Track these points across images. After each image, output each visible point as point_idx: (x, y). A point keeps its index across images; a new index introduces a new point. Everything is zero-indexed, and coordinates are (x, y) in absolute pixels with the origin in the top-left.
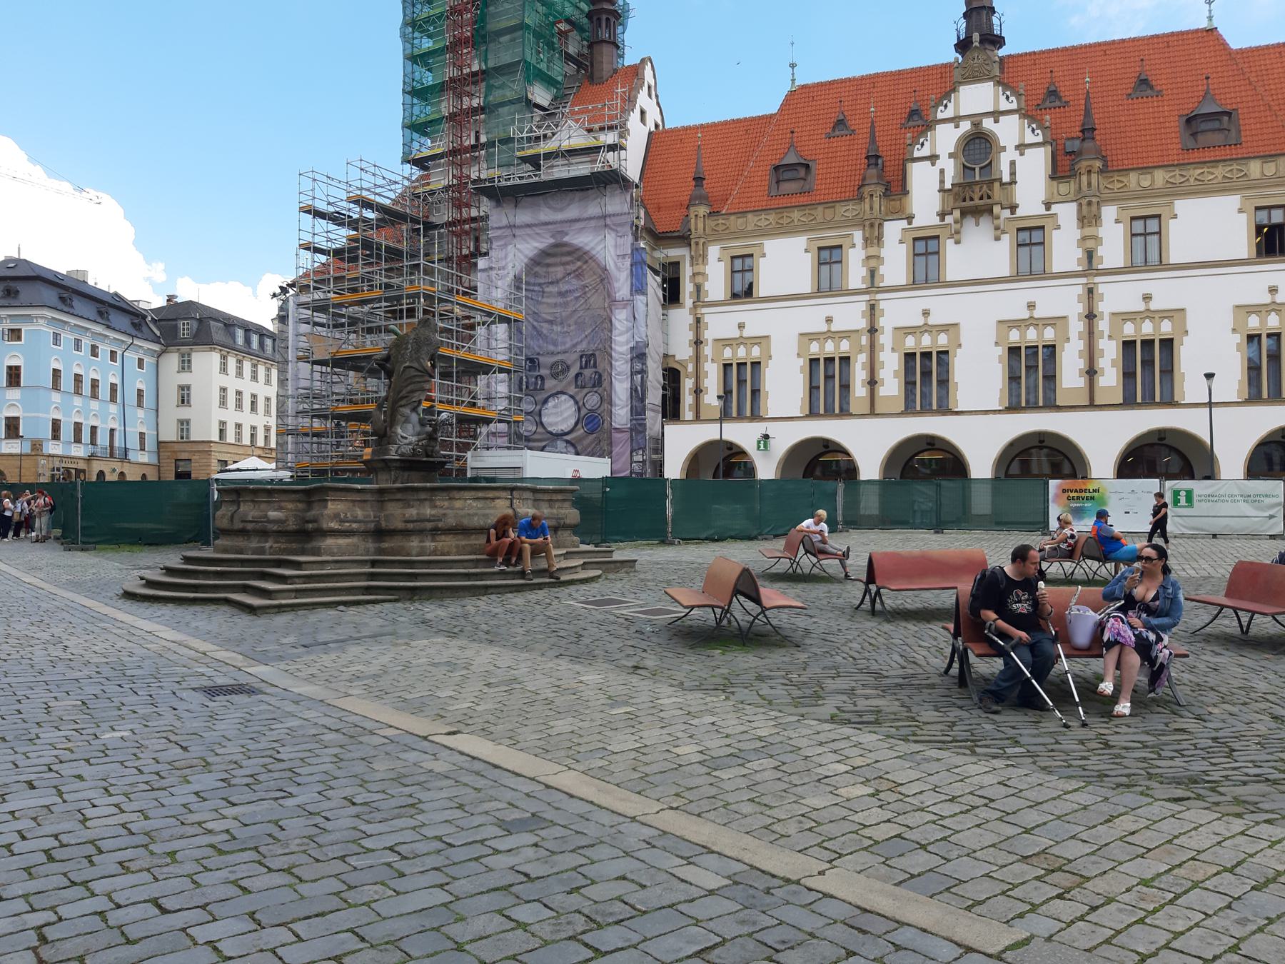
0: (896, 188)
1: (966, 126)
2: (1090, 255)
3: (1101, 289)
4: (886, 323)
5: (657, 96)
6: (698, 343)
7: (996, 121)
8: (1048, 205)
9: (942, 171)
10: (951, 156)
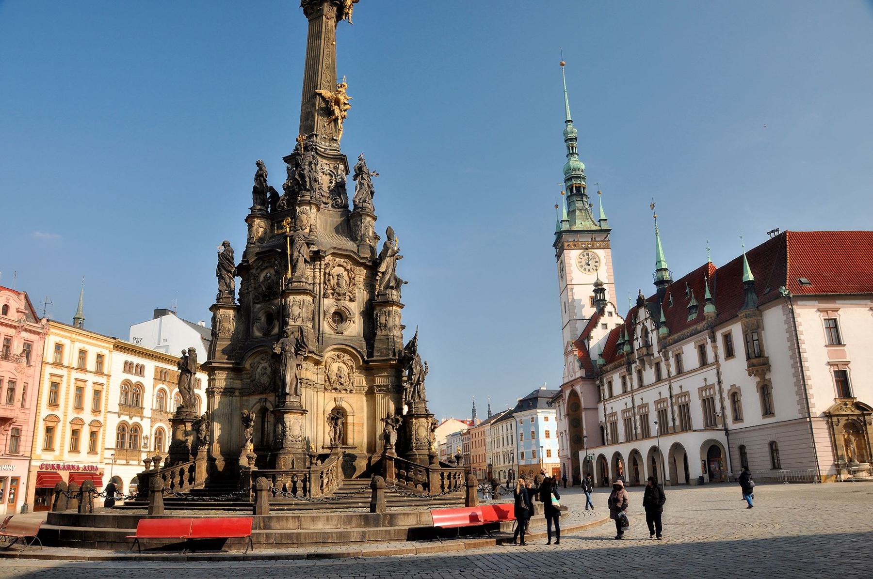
3: (673, 385)
4: (636, 404)
8: (659, 352)
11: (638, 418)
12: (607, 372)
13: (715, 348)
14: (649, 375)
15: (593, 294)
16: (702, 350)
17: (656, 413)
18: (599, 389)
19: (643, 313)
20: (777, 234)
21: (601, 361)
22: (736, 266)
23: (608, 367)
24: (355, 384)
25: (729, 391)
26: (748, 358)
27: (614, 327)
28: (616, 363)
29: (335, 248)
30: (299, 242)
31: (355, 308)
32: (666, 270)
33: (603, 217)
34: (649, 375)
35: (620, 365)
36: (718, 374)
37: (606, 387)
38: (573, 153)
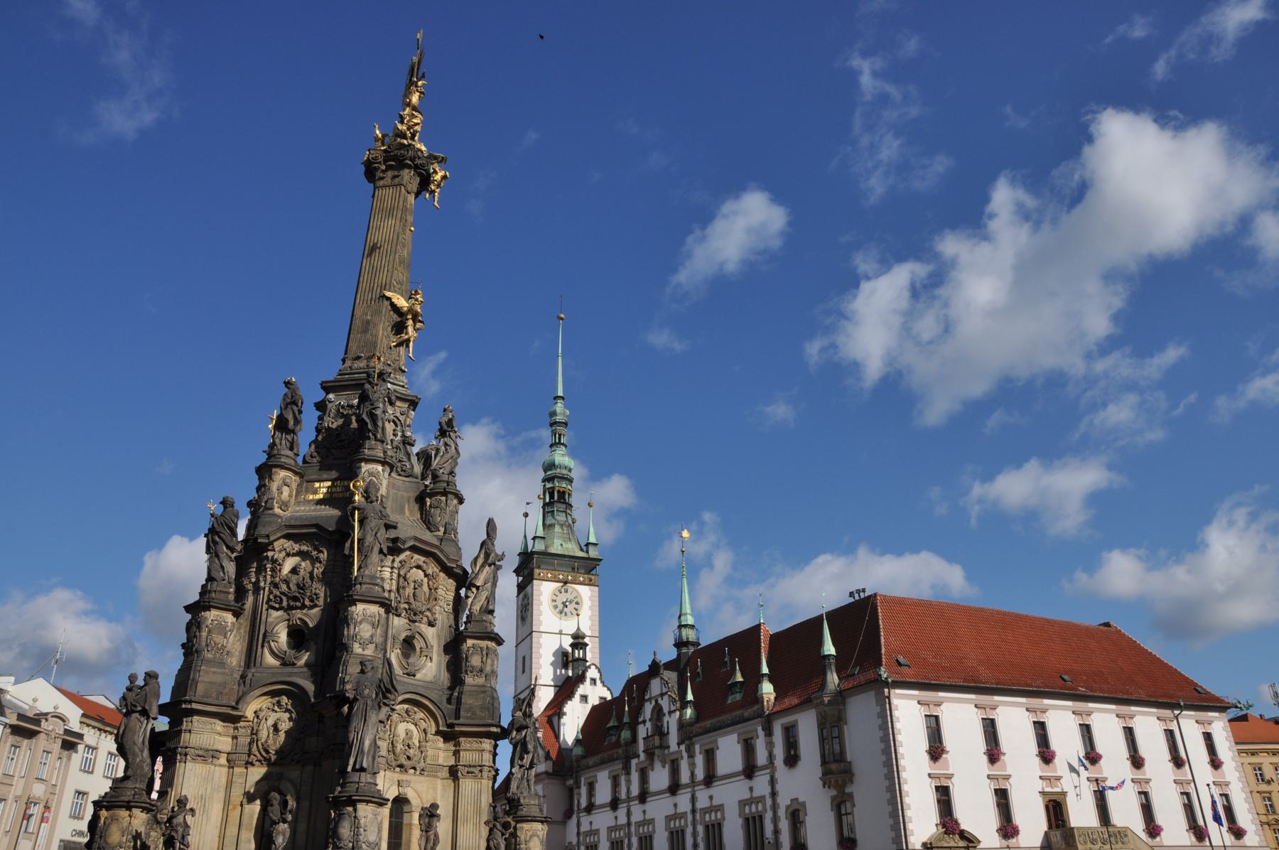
0: (634, 739)
2: (693, 774)
3: (698, 794)
4: (634, 819)
5: (602, 682)
6: (578, 834)
8: (679, 744)
11: (635, 840)
12: (588, 767)
13: (770, 746)
14: (659, 778)
15: (570, 650)
16: (748, 749)
17: (666, 834)
18: (571, 793)
19: (655, 686)
20: (862, 595)
21: (578, 751)
22: (810, 629)
23: (591, 761)
24: (428, 761)
25: (788, 807)
26: (824, 762)
27: (597, 702)
28: (605, 755)
29: (416, 539)
30: (373, 523)
31: (433, 637)
32: (692, 627)
33: (592, 539)
34: (659, 778)
35: (611, 760)
36: (773, 782)
37: (584, 790)
38: (560, 443)
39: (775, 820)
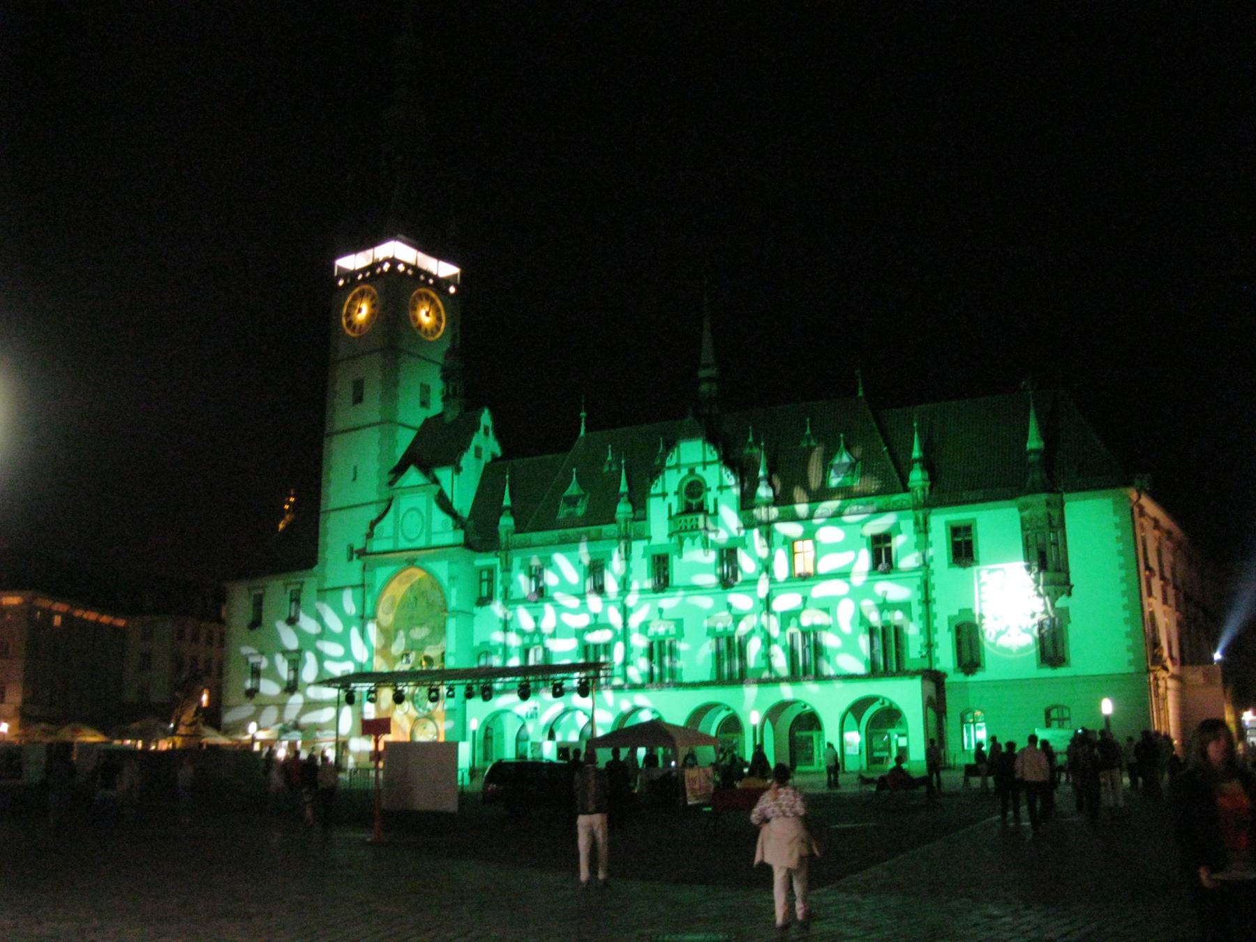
1: (685, 472)
7: (705, 469)
9: (670, 506)
10: (676, 493)
18: (488, 577)
25: (950, 619)
36: (926, 587)
39: (928, 630)
